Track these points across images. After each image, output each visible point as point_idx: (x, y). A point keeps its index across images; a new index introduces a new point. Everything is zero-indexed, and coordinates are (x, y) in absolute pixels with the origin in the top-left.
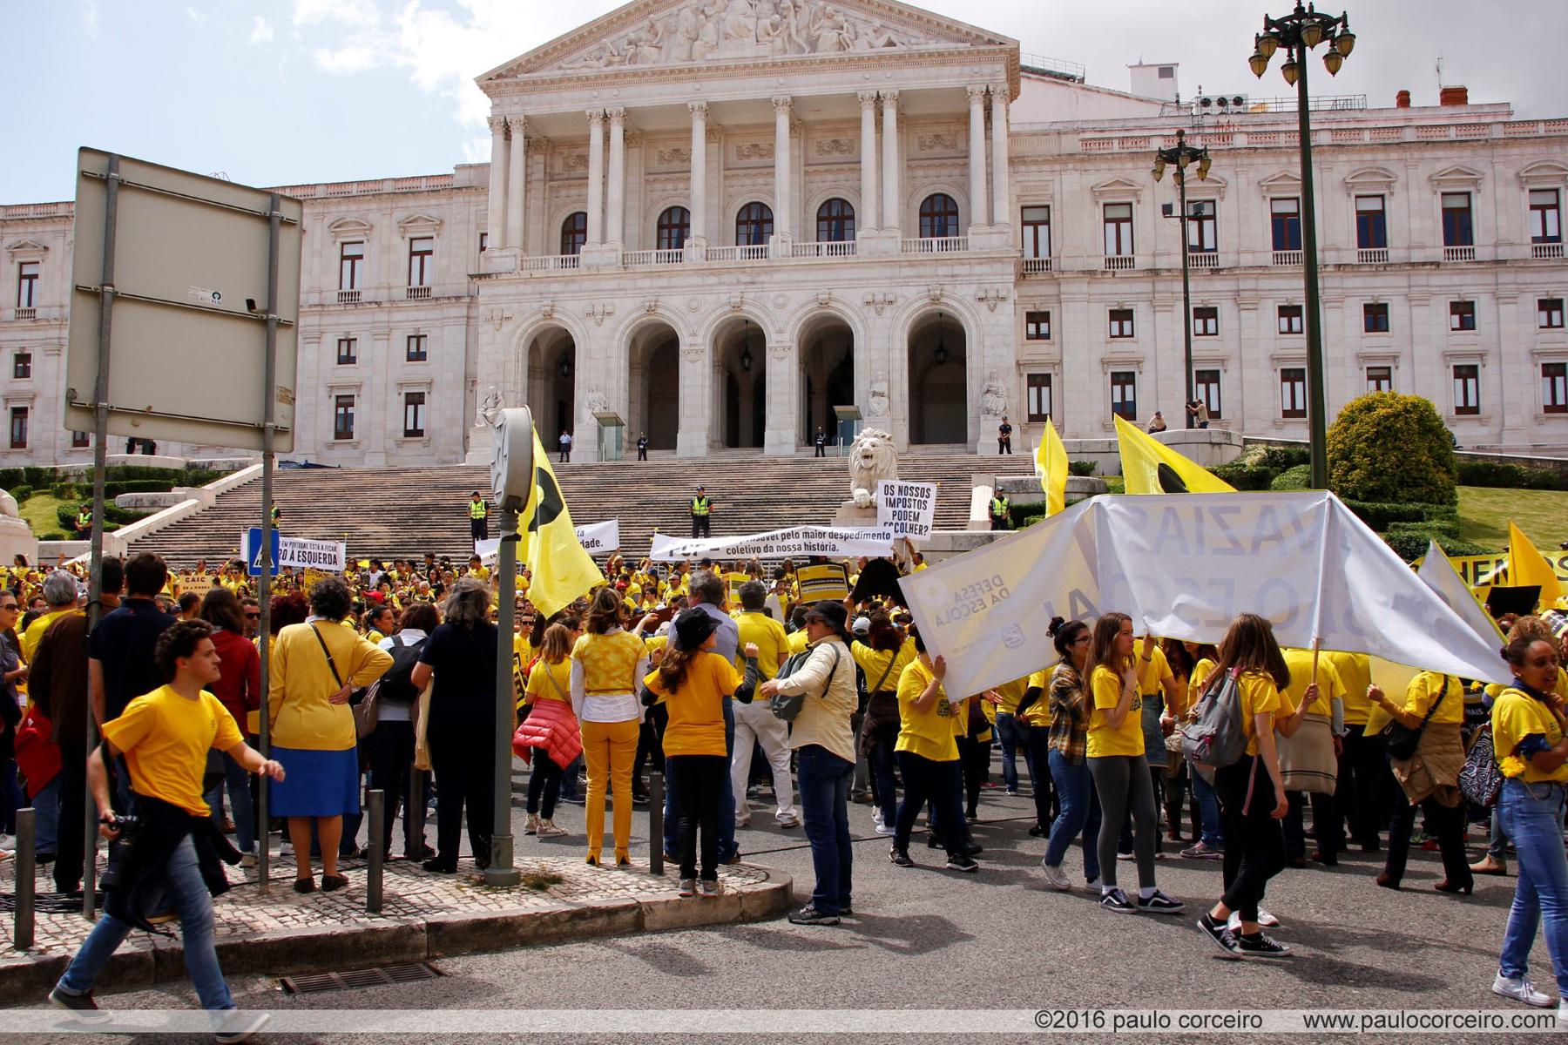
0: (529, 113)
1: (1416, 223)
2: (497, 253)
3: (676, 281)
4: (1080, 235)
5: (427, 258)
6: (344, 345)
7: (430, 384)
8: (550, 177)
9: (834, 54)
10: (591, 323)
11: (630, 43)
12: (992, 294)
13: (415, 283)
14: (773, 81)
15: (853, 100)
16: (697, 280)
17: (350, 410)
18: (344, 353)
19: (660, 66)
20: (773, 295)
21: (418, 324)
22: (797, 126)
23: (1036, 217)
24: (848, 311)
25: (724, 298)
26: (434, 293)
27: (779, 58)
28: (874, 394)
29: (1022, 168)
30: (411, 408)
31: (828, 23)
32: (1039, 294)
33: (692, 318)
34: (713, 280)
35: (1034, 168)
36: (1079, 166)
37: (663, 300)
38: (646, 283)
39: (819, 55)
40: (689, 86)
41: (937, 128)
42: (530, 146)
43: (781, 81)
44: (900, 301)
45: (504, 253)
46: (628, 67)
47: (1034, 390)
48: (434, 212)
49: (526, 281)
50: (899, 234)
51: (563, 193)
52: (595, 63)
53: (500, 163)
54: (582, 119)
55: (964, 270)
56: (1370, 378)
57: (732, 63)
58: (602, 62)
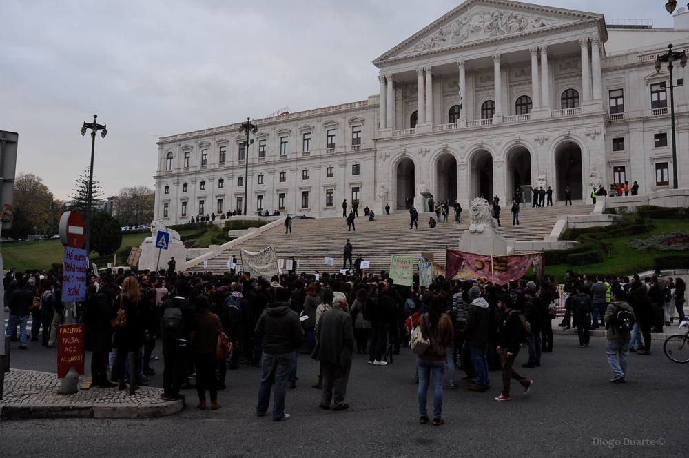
3: (455, 136)
4: (639, 100)
6: (329, 170)
7: (361, 183)
8: (405, 97)
9: (518, 33)
10: (421, 156)
11: (432, 40)
12: (594, 132)
15: (527, 53)
17: (332, 195)
18: (329, 173)
20: (495, 139)
22: (503, 67)
23: (616, 93)
24: (527, 144)
25: (475, 142)
27: (494, 38)
28: (540, 179)
29: (609, 73)
30: (354, 193)
32: (617, 131)
34: (470, 135)
35: (615, 72)
36: (637, 69)
37: (449, 145)
38: (442, 138)
39: (511, 34)
40: (457, 55)
41: (565, 60)
42: (396, 86)
43: (496, 48)
44: (551, 139)
46: (432, 50)
47: (617, 174)
49: (395, 140)
50: (549, 109)
51: (411, 103)
53: (383, 94)
54: (414, 73)
55: (579, 122)
57: (474, 43)
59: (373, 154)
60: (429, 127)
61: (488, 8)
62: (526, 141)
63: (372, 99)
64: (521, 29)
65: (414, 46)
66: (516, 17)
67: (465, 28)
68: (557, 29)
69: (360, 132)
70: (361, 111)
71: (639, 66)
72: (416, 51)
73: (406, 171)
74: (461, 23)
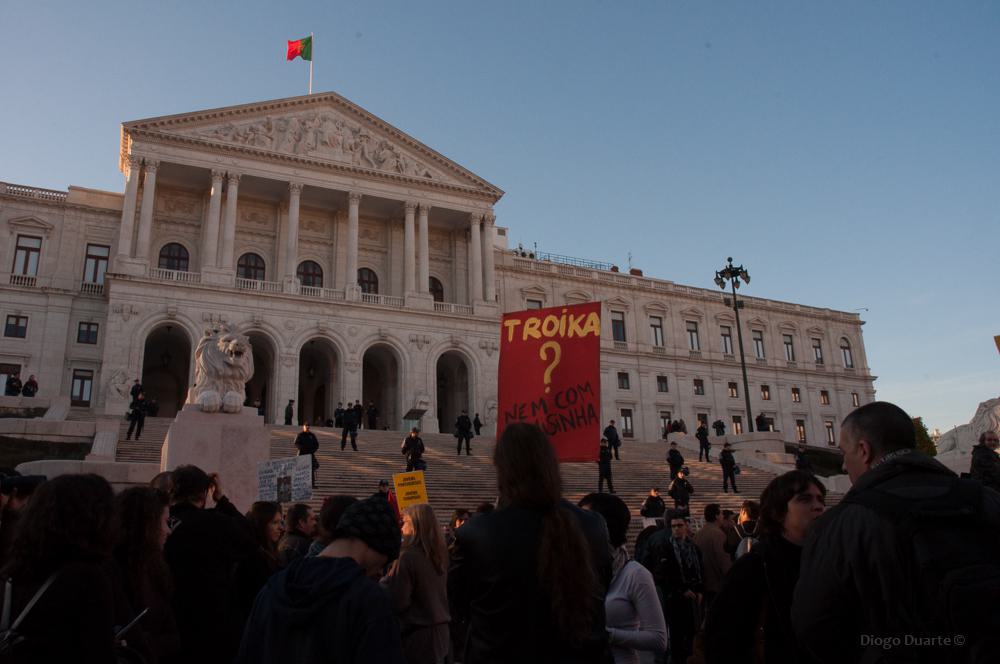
0: (164, 160)
1: (677, 335)
2: (129, 260)
3: (277, 305)
5: (33, 255)
9: (392, 172)
11: (251, 129)
12: (491, 345)
13: (19, 271)
14: (349, 181)
16: (290, 307)
19: (273, 151)
21: (20, 307)
24: (400, 345)
25: (313, 323)
26: (40, 283)
27: (356, 165)
31: (388, 152)
33: (288, 334)
34: (305, 309)
36: (514, 275)
37: (267, 318)
38: (253, 303)
39: (384, 171)
45: (135, 261)
46: (248, 146)
48: (45, 219)
51: (164, 226)
52: (225, 138)
55: (471, 327)
56: (662, 417)
57: (326, 163)
58: (229, 138)
59: (68, 302)
60: (229, 278)
61: (347, 118)
62: (400, 341)
63: (79, 195)
64: (398, 168)
65: (215, 127)
66: (391, 149)
67: (311, 136)
68: (448, 187)
69: (38, 250)
70: (46, 210)
71: (516, 271)
72: (220, 139)
73: (167, 354)
74: (304, 124)
